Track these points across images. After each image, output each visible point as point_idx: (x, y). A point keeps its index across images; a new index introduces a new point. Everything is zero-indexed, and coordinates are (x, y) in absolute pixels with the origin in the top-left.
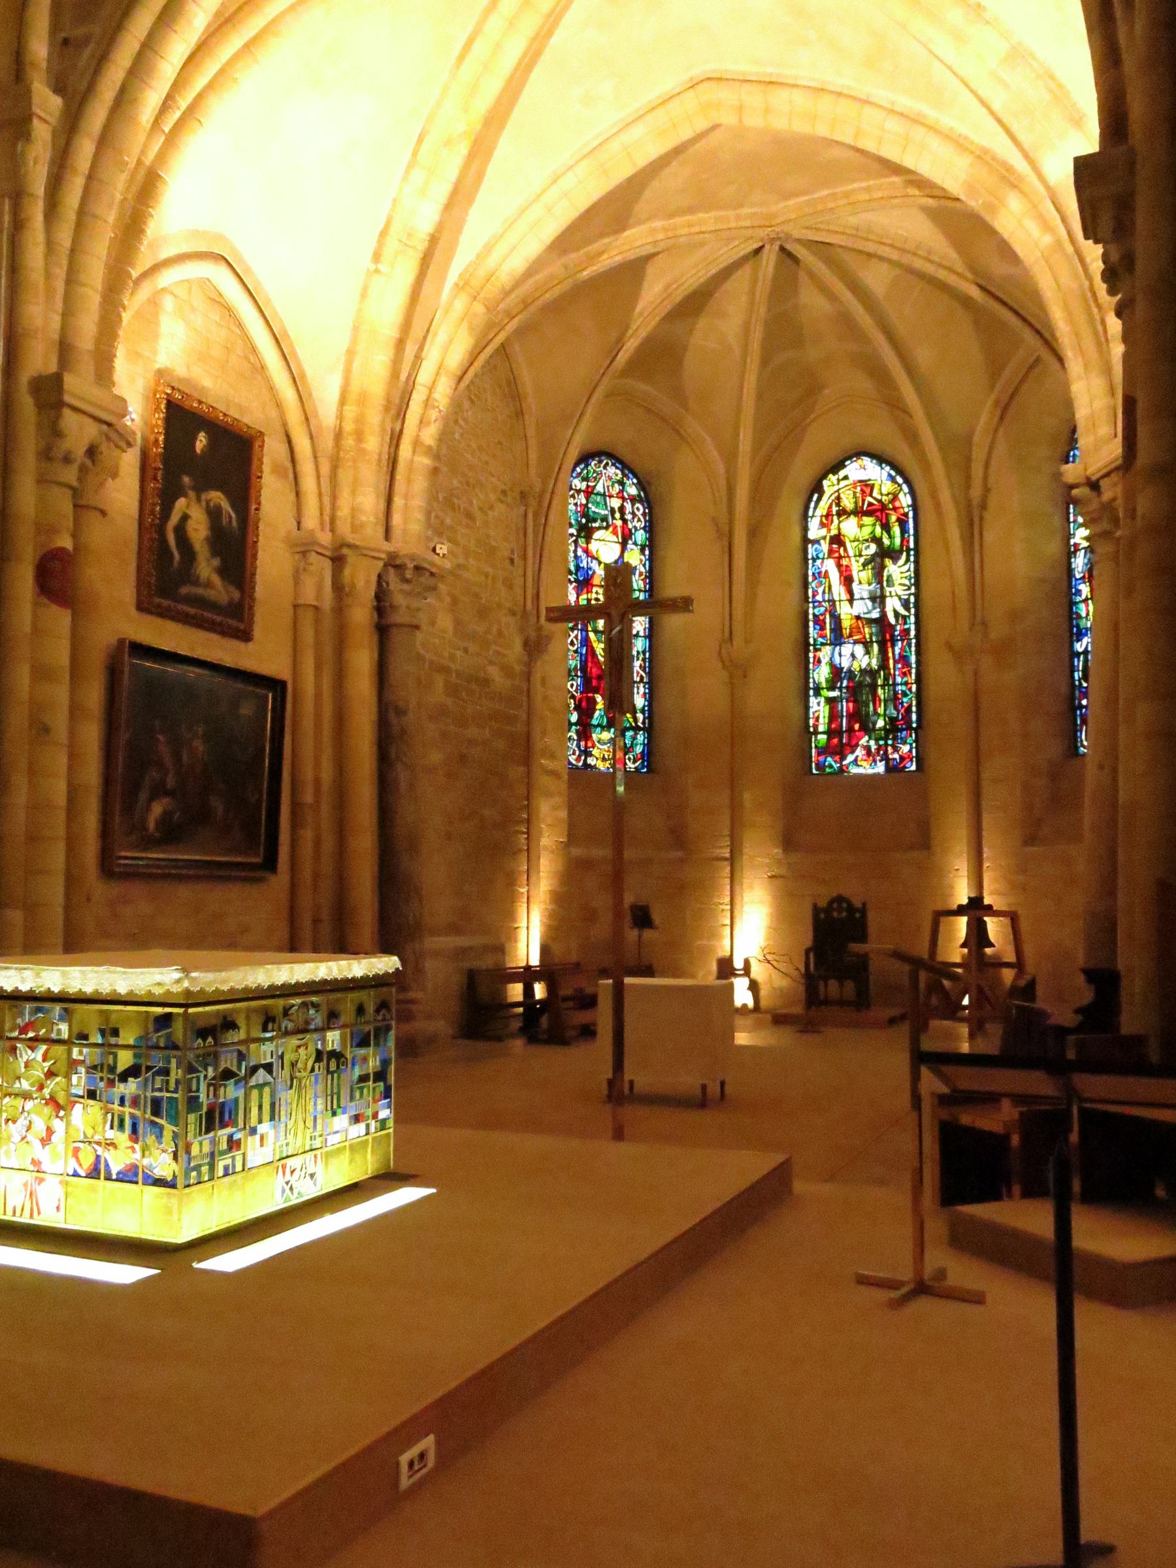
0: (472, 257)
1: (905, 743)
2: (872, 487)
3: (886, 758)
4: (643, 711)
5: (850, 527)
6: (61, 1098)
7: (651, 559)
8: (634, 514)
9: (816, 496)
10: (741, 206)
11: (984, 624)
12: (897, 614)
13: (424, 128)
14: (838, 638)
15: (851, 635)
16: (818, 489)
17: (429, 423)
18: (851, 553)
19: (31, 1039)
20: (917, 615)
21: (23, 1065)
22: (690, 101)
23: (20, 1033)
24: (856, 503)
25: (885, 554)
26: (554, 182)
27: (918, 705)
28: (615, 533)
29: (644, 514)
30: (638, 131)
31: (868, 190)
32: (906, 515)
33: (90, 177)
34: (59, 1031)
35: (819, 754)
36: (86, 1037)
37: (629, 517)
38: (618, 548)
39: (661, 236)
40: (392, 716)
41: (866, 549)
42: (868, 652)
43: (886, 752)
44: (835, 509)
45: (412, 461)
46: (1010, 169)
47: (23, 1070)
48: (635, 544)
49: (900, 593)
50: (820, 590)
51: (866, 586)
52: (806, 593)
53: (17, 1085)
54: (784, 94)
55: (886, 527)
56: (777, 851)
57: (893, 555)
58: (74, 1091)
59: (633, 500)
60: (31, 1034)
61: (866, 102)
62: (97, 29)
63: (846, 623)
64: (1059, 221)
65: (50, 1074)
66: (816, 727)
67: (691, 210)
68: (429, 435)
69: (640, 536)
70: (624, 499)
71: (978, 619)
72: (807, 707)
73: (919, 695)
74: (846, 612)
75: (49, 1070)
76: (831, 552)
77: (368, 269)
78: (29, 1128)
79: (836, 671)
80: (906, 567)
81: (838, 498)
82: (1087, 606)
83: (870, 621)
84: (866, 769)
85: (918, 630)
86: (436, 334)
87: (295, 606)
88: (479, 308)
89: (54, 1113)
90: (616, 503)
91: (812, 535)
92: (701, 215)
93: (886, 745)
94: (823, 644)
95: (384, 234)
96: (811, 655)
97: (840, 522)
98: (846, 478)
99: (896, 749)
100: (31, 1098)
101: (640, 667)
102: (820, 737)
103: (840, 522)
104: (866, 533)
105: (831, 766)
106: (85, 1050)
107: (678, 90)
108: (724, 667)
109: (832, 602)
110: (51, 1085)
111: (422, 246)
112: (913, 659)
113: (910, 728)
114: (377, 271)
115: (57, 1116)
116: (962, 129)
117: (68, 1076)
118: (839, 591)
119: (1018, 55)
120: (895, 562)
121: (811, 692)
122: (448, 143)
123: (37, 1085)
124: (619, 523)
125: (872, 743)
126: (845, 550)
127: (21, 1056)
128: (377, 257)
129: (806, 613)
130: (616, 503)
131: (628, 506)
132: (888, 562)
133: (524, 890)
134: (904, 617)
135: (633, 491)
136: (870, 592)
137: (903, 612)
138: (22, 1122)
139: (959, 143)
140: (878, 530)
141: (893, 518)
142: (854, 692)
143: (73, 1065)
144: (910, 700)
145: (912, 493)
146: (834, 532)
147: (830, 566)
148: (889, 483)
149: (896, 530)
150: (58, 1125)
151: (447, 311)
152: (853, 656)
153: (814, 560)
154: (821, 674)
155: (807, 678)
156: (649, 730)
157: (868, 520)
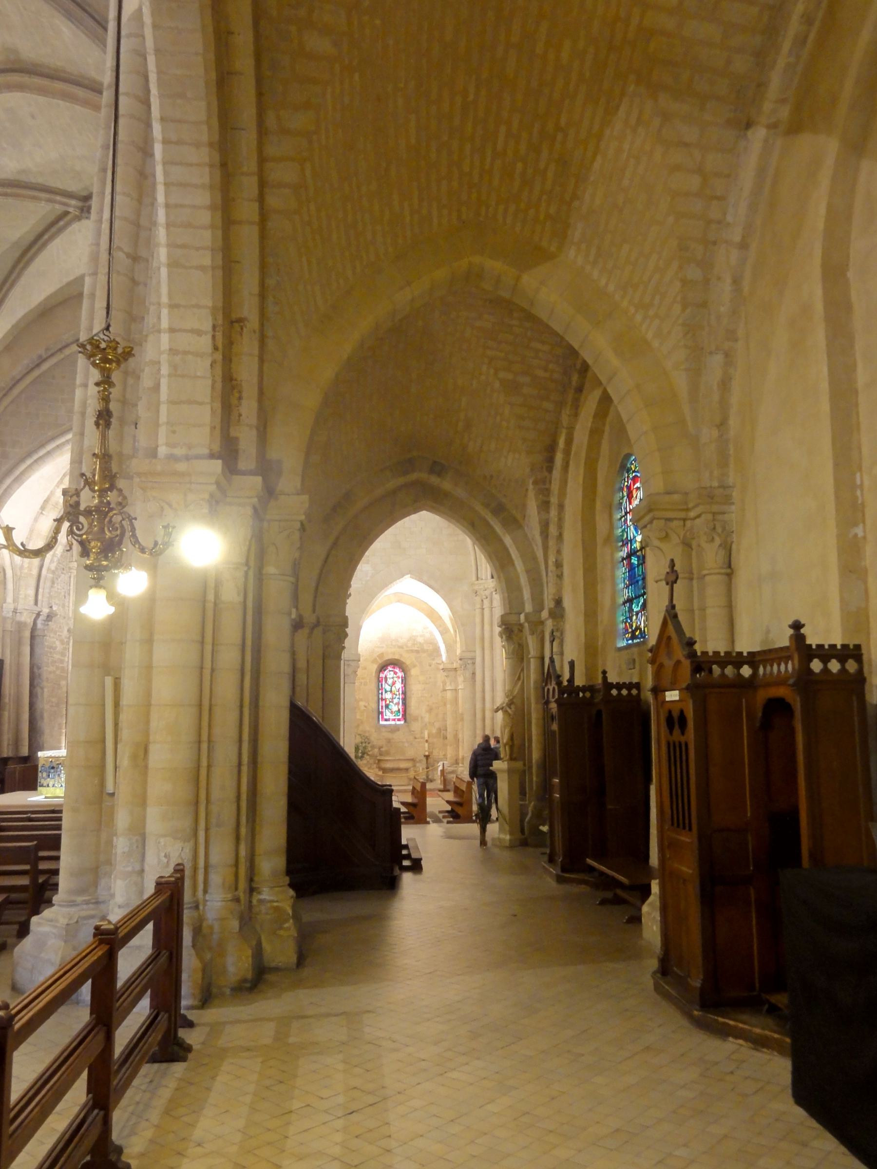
17: (54, 562)
40: (36, 670)
45: (46, 576)
68: (53, 567)
77: (38, 512)
95: (46, 501)
114: (42, 513)
128: (43, 508)
133: (64, 731)
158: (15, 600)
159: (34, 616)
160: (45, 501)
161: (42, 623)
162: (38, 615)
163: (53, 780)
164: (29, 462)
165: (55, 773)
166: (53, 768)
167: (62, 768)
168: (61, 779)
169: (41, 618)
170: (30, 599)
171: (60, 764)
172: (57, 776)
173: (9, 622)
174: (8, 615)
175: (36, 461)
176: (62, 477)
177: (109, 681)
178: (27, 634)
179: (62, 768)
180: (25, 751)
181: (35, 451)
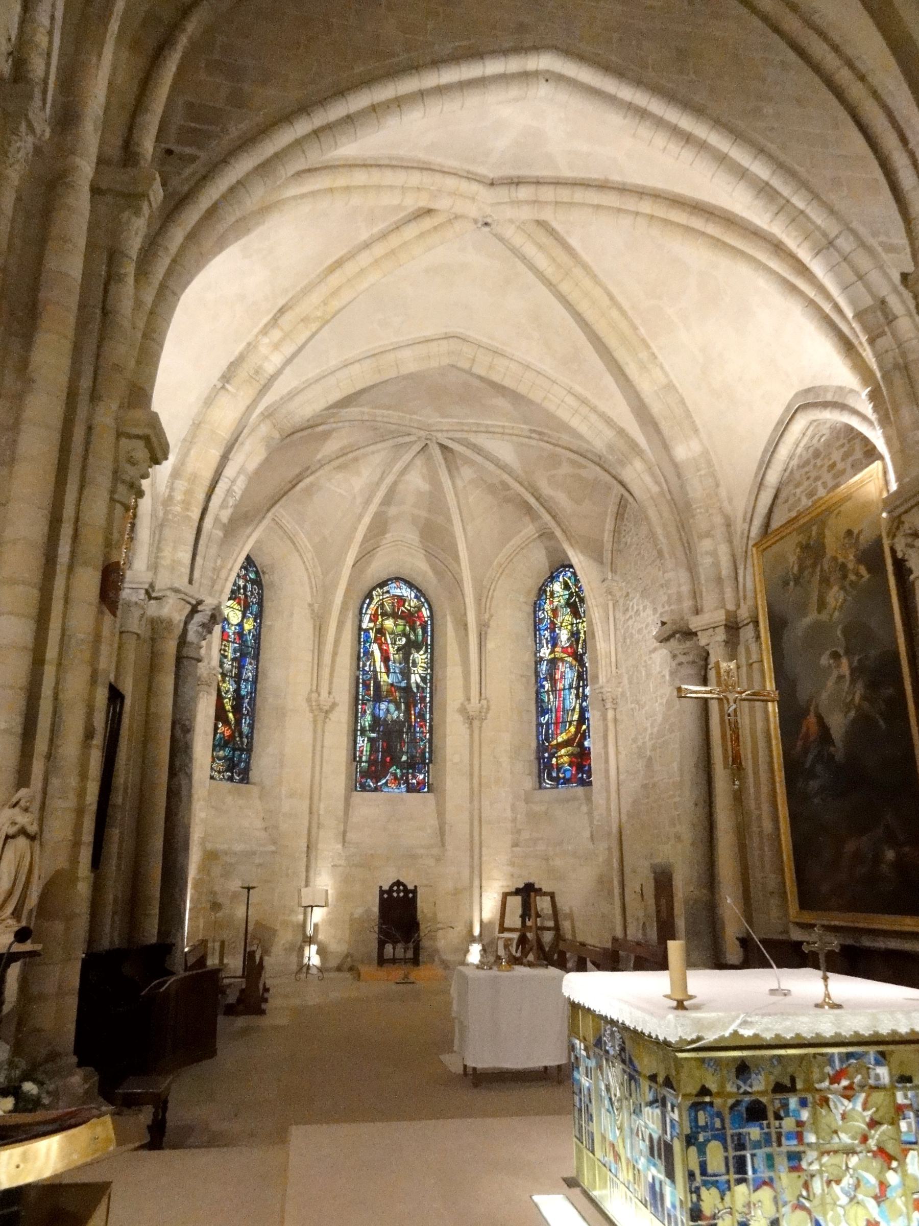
0: (278, 398)
1: (421, 773)
2: (405, 601)
3: (407, 782)
4: (247, 737)
5: (389, 623)
6: (890, 1148)
8: (252, 594)
9: (367, 601)
10: (415, 413)
11: (486, 699)
12: (418, 686)
13: (287, 303)
14: (378, 698)
15: (386, 697)
16: (369, 596)
17: (227, 507)
18: (389, 642)
19: (845, 1088)
20: (431, 688)
21: (839, 1117)
22: (444, 346)
23: (832, 1083)
24: (394, 609)
26: (346, 366)
27: (430, 747)
28: (239, 604)
29: (258, 594)
30: (407, 353)
31: (503, 427)
32: (426, 622)
33: (174, 261)
34: (877, 1077)
35: (362, 777)
36: (909, 1079)
37: (249, 594)
38: (240, 614)
39: (366, 417)
40: (179, 733)
41: (400, 640)
42: (398, 708)
43: (407, 778)
44: (380, 611)
46: (637, 445)
47: (840, 1122)
48: (251, 613)
49: (421, 672)
50: (368, 663)
51: (398, 665)
52: (359, 665)
53: (836, 1140)
54: (506, 362)
55: (413, 629)
56: (340, 846)
57: (418, 646)
58: (904, 1138)
59: (253, 582)
60: (845, 1083)
61: (554, 382)
62: (203, 155)
63: (384, 688)
64: (662, 480)
65: (874, 1124)
66: (361, 757)
67: (389, 408)
68: (225, 516)
69: (255, 608)
70: (247, 581)
71: (483, 695)
72: (355, 742)
75: (872, 1119)
76: (376, 640)
78: (857, 1186)
80: (424, 657)
81: (382, 604)
82: (549, 695)
83: (399, 689)
85: (431, 697)
86: (242, 443)
87: (121, 633)
88: (277, 435)
89: (885, 1165)
90: (241, 583)
91: (364, 626)
92: (390, 412)
93: (408, 773)
94: (368, 700)
96: (360, 707)
97: (383, 620)
98: (388, 592)
99: (414, 777)
100: (854, 1152)
101: (248, 703)
102: (363, 764)
103: (383, 620)
104: (400, 628)
105: (369, 786)
106: (910, 1094)
107: (437, 337)
108: (312, 711)
109: (375, 672)
110: (876, 1135)
111: (263, 382)
112: (428, 716)
113: (423, 762)
115: (890, 1168)
116: (611, 413)
117: (894, 1123)
118: (379, 665)
119: (670, 387)
120: (418, 652)
121: (359, 733)
122: (305, 320)
123: (859, 1137)
124: (242, 597)
125: (398, 771)
126: (386, 639)
127: (836, 1107)
128: (226, 378)
129: (358, 678)
130: (241, 583)
131: (249, 586)
132: (413, 651)
134: (423, 688)
135: (252, 576)
136: (401, 669)
137: (422, 684)
138: (847, 1181)
139: (609, 421)
140: (408, 628)
141: (418, 623)
143: (900, 1110)
145: (430, 608)
146: (378, 626)
147: (375, 648)
148: (415, 600)
149: (420, 631)
150: (892, 1178)
151: (253, 430)
152: (388, 710)
153: (365, 642)
154: (367, 720)
155: (356, 722)
157: (400, 622)
158: (154, 567)
159: (188, 608)
160: (232, 364)
161: (197, 631)
162: (194, 610)
163: (765, 1194)
164: (302, 127)
165: (774, 1149)
166: (756, 1113)
167: (805, 1115)
168: (806, 1186)
169: (198, 618)
170: (183, 570)
171: (792, 1089)
172: (782, 1164)
173: (137, 613)
174: (134, 599)
175: (316, 133)
176: (275, 315)
178: (171, 647)
179: (805, 1115)
180: (151, 932)
181: (323, 101)
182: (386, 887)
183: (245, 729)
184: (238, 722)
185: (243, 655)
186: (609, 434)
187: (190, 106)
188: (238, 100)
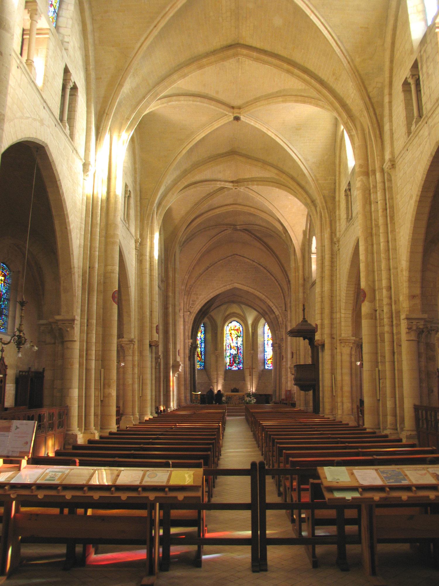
5: (233, 332)
7: (205, 336)
14: (231, 349)
16: (228, 325)
25: (238, 336)
57: (239, 337)
59: (203, 327)
63: (232, 347)
73: (243, 358)
74: (232, 345)
79: (231, 354)
84: (235, 369)
118: (231, 342)
132: (238, 338)
139: (262, 309)
140: (237, 333)
141: (239, 331)
142: (233, 357)
144: (241, 359)
147: (230, 337)
149: (240, 333)
154: (228, 354)
156: (204, 362)
157: (236, 331)
177: (333, 376)
182: (232, 389)
183: (203, 358)
184: (201, 357)
185: (202, 343)
186: (262, 311)
187: (192, 300)
188: (197, 298)
